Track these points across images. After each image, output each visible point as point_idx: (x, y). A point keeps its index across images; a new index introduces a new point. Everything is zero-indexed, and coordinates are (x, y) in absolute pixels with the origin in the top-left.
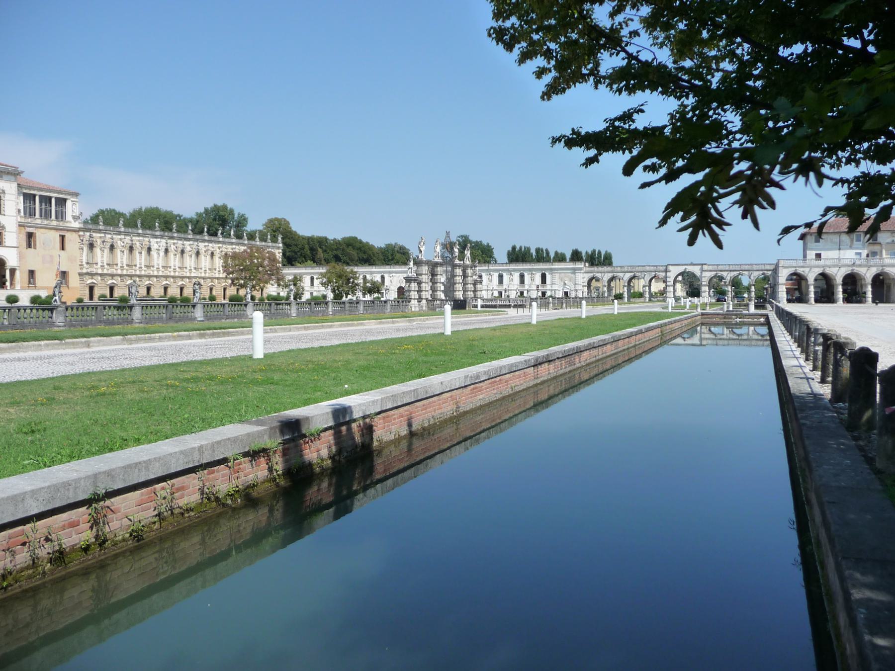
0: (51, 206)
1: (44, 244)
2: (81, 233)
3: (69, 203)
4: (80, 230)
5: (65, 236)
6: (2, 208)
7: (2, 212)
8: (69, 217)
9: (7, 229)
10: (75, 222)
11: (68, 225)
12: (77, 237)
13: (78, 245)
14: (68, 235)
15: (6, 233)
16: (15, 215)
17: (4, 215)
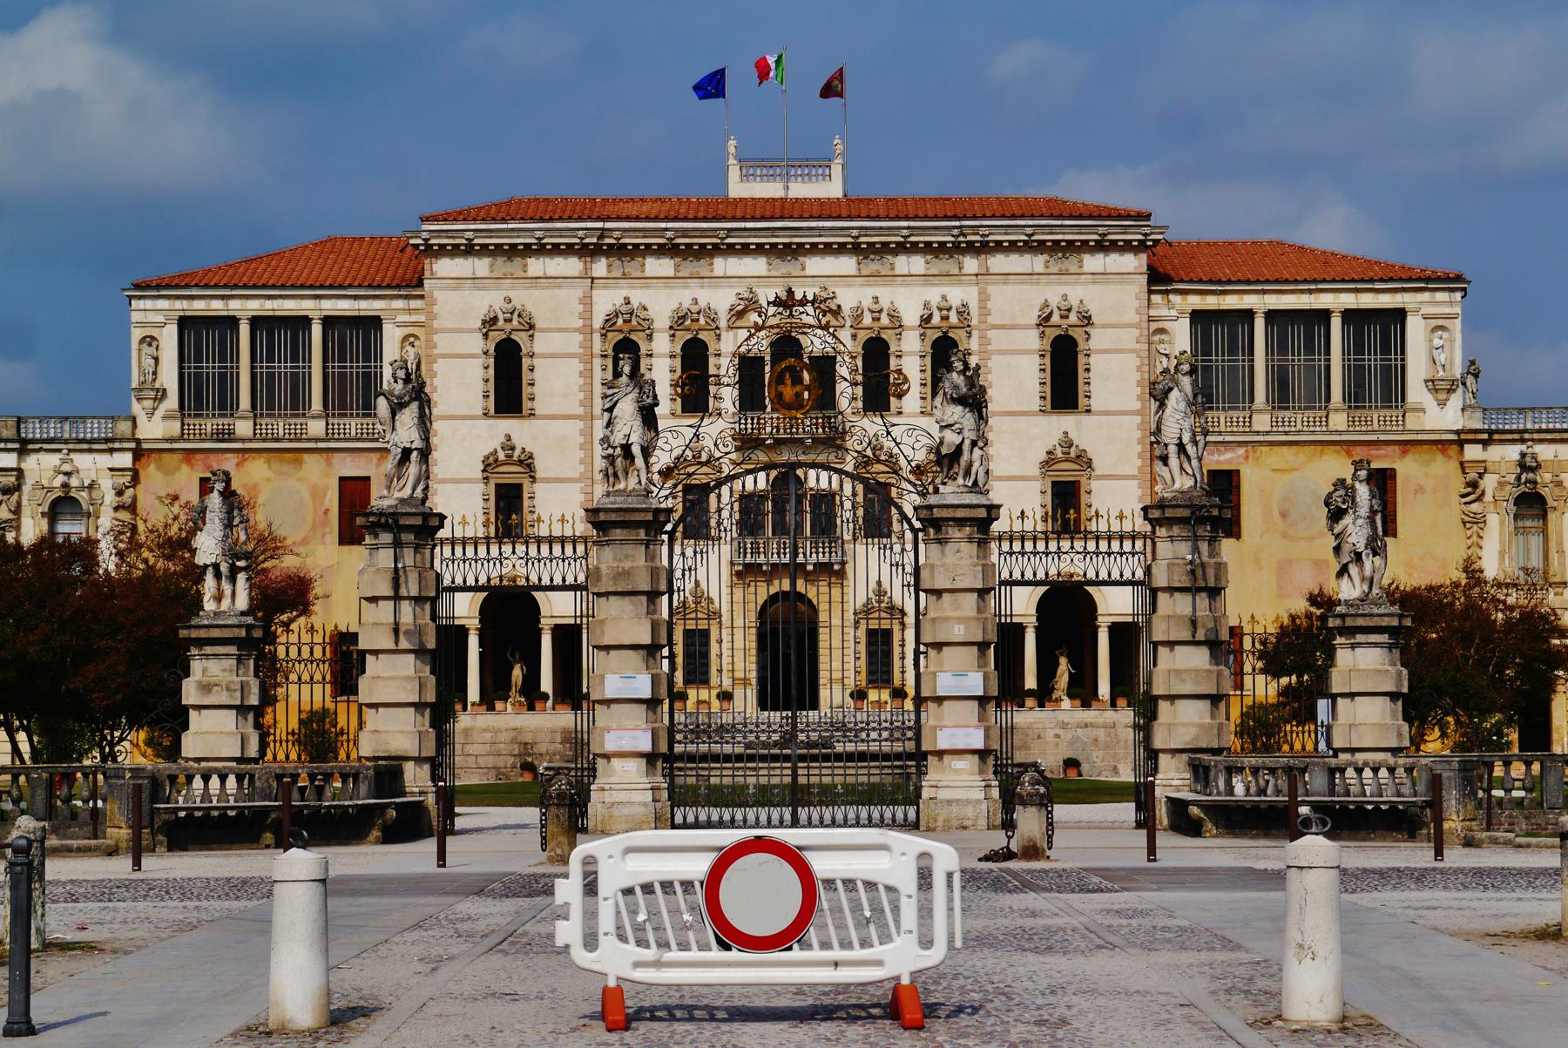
0: (1328, 352)
1: (1284, 515)
2: (1473, 452)
3: (1415, 329)
4: (1461, 439)
5: (1393, 470)
6: (1081, 381)
7: (1082, 401)
8: (1416, 391)
9: (1100, 466)
10: (1442, 404)
11: (1412, 422)
12: (1453, 466)
13: (1455, 507)
14: (1407, 469)
15: (1095, 485)
16: (1137, 405)
17: (1088, 411)
